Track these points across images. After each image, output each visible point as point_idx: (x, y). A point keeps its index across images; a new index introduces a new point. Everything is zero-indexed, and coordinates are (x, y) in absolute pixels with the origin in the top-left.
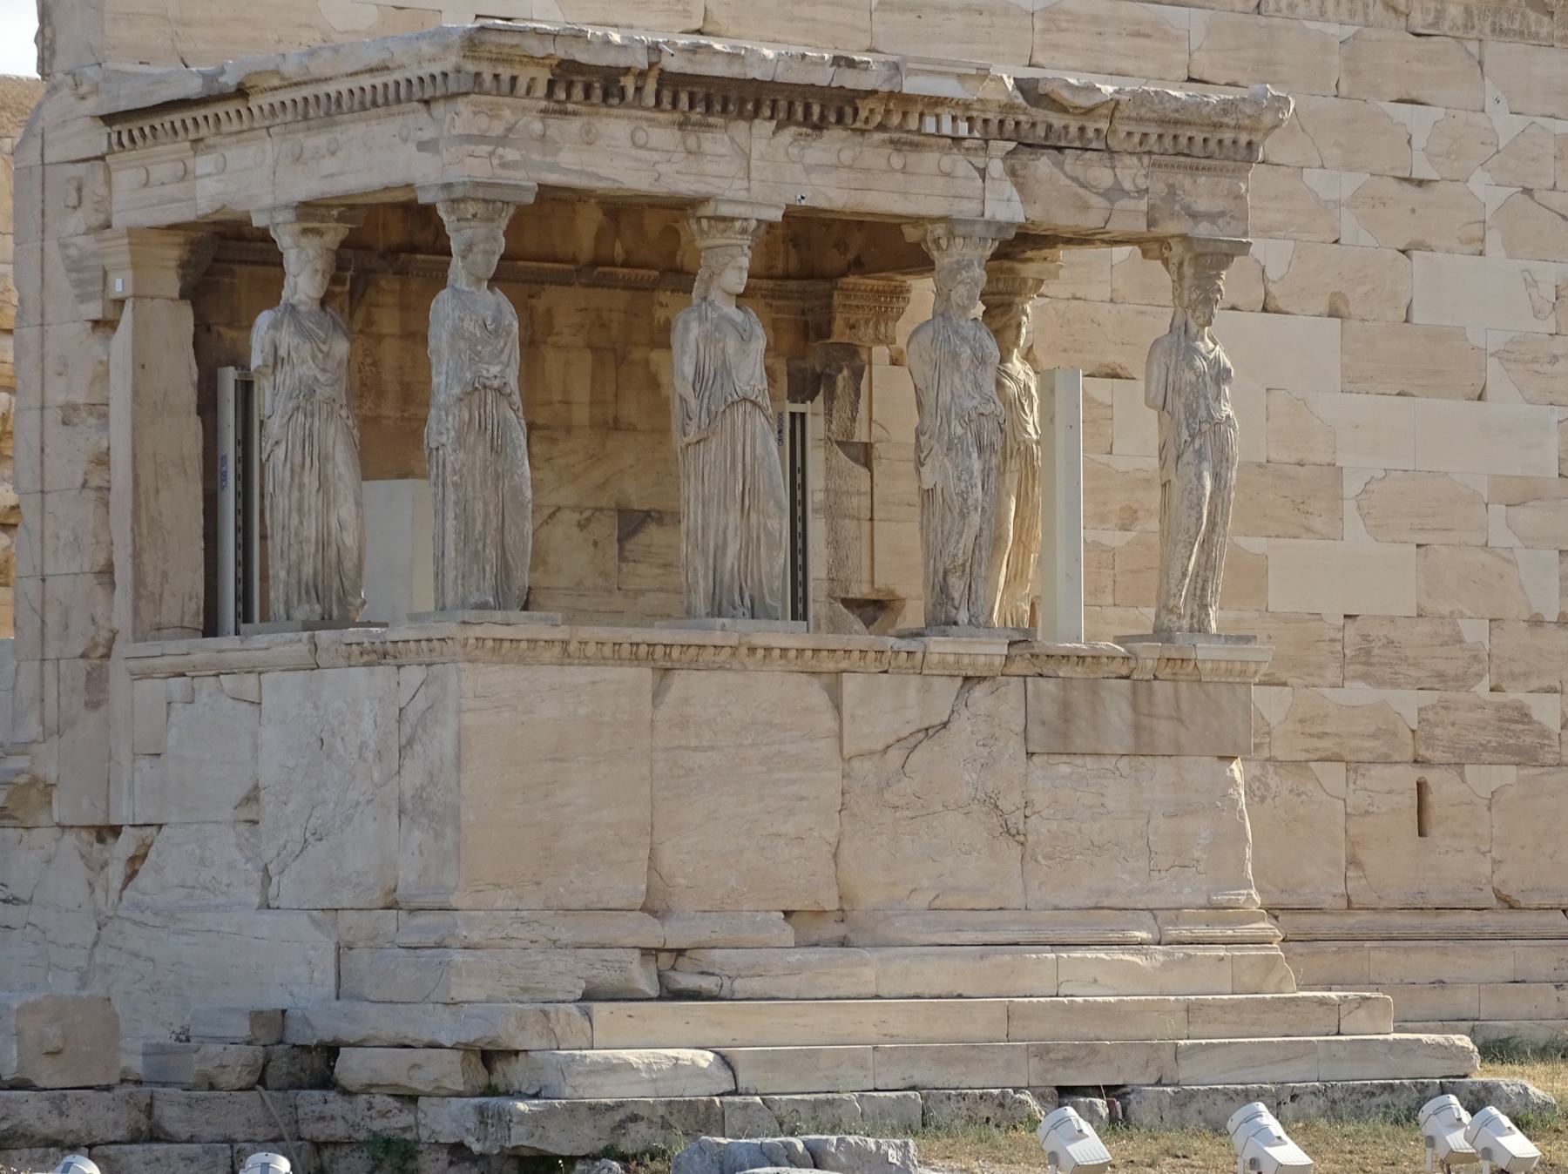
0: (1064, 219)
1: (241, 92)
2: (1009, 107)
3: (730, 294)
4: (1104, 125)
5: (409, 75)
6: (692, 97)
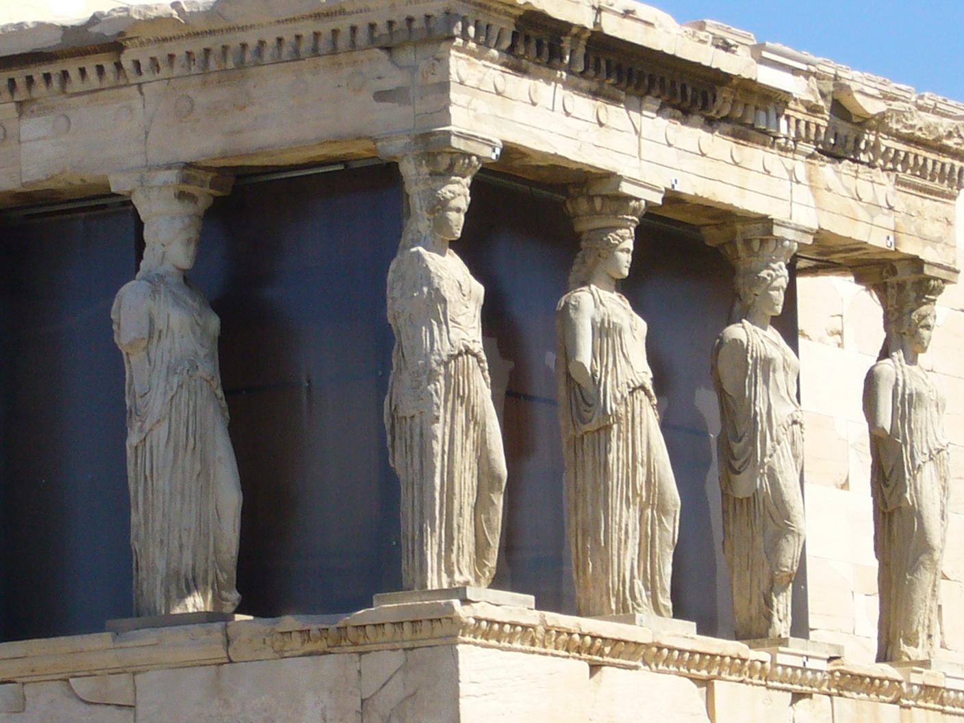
0: (843, 228)
1: (115, 46)
2: (813, 109)
3: (613, 278)
4: (872, 138)
5: (373, 20)
6: (608, 63)
